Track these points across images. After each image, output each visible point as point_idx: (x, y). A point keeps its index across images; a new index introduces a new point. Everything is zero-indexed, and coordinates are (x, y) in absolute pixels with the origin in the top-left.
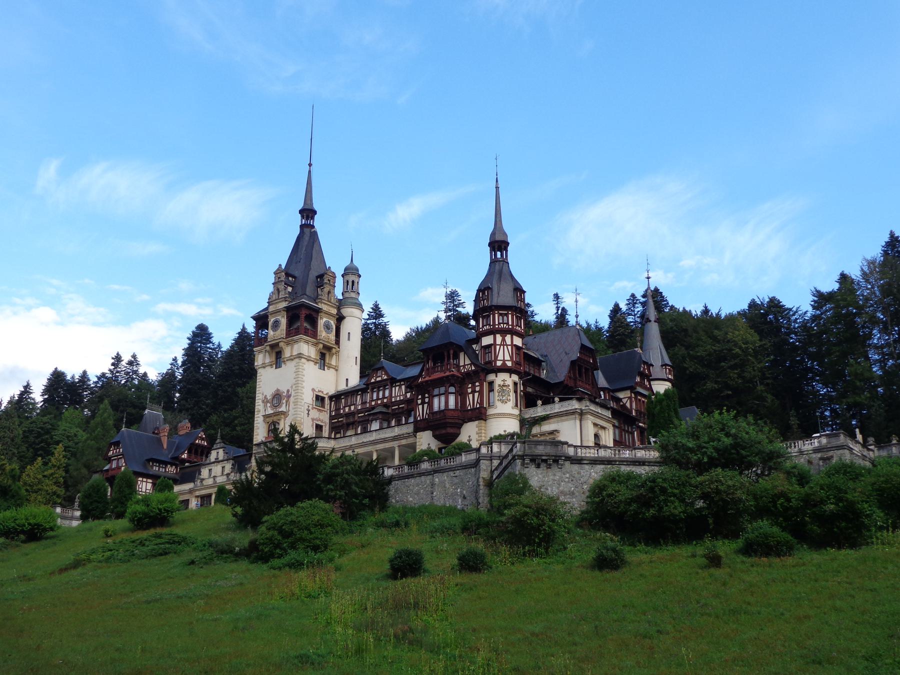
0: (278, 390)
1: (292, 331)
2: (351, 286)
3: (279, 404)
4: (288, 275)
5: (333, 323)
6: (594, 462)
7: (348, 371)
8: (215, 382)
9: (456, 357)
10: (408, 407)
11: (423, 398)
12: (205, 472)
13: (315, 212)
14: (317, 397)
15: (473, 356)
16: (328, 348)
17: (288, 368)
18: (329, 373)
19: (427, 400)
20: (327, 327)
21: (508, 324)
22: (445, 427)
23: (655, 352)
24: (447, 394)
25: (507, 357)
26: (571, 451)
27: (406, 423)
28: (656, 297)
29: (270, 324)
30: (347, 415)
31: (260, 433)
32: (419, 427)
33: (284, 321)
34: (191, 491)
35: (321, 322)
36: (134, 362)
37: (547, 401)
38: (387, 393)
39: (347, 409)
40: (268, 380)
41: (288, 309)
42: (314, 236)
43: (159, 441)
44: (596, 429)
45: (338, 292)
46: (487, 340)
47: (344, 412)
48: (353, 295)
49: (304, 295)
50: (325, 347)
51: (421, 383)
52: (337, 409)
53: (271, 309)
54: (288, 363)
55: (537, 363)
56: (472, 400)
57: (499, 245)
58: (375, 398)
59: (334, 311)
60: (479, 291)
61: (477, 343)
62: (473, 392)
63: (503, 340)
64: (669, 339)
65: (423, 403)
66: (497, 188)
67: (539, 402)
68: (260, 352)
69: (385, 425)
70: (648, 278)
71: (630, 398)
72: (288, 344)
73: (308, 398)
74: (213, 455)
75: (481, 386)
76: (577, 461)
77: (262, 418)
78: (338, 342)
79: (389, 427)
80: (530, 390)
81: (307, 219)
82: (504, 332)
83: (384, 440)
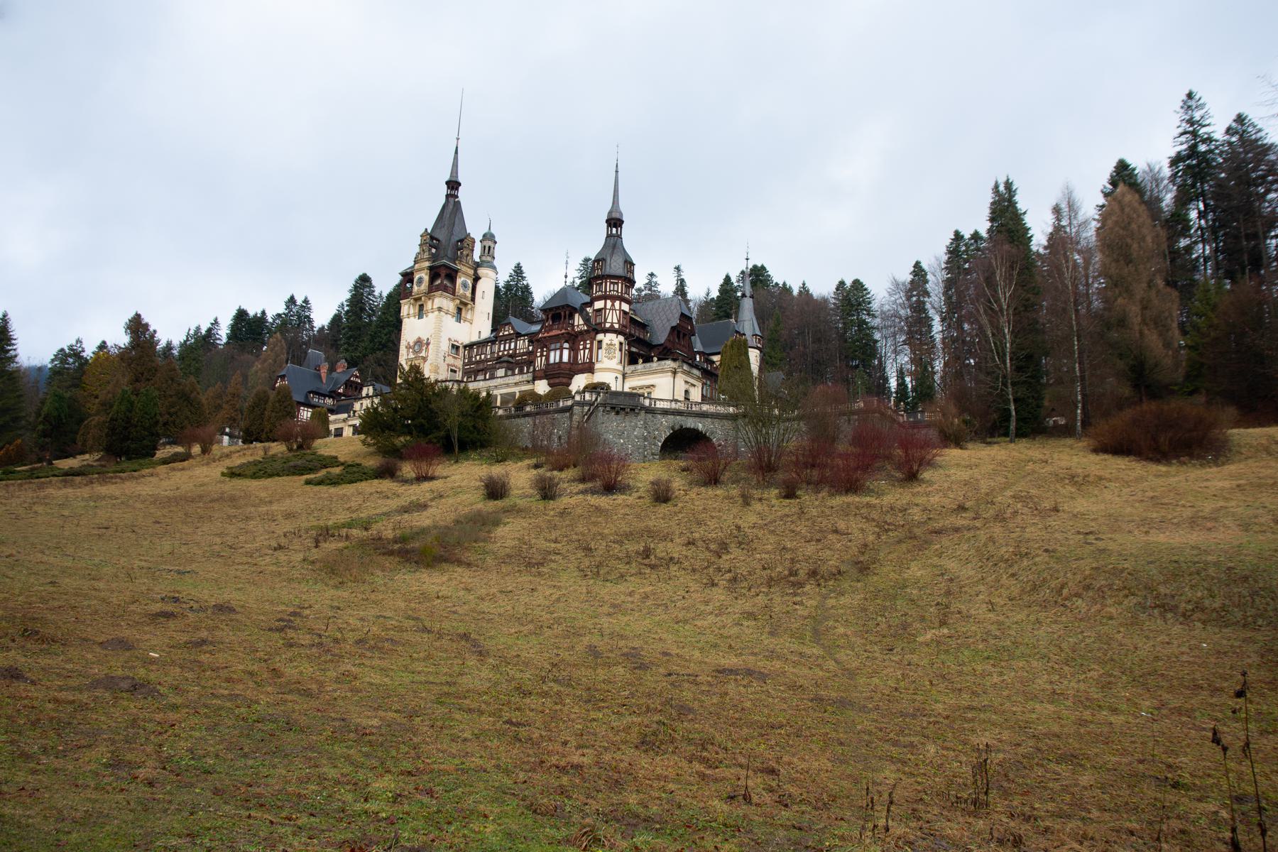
1: (432, 289)
2: (488, 251)
3: (420, 351)
4: (432, 238)
5: (470, 282)
6: (665, 412)
7: (479, 325)
8: (369, 328)
9: (571, 317)
14: (453, 346)
16: (466, 304)
17: (431, 318)
18: (464, 325)
20: (465, 285)
22: (559, 376)
23: (747, 322)
24: (561, 349)
25: (615, 320)
26: (647, 403)
28: (758, 276)
30: (477, 363)
33: (426, 278)
34: (344, 421)
35: (459, 281)
40: (413, 328)
41: (431, 268)
42: (458, 205)
43: (320, 377)
44: (687, 386)
46: (599, 305)
47: (476, 359)
48: (489, 259)
49: (447, 256)
50: (462, 303)
52: (470, 358)
54: (430, 315)
55: (643, 326)
56: (583, 355)
57: (615, 222)
58: (503, 349)
59: (472, 272)
62: (585, 348)
64: (761, 315)
73: (445, 347)
74: (364, 393)
75: (592, 344)
76: (651, 411)
78: (473, 299)
79: (514, 374)
80: (634, 349)
82: (613, 298)
83: (508, 385)
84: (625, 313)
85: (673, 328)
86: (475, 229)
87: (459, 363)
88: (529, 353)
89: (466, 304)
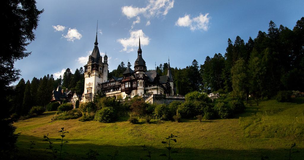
10: (120, 86)
11: (123, 85)
12: (72, 100)
13: (98, 44)
15: (134, 76)
16: (101, 73)
18: (101, 79)
25: (142, 76)
27: (119, 90)
31: (85, 92)
32: (122, 91)
35: (99, 68)
36: (52, 75)
37: (150, 86)
38: (114, 83)
41: (92, 65)
50: (100, 73)
52: (103, 87)
53: (88, 65)
55: (148, 78)
56: (134, 85)
57: (140, 52)
59: (102, 65)
60: (136, 62)
61: (135, 73)
62: (134, 84)
63: (141, 73)
65: (123, 86)
66: (140, 40)
67: (148, 86)
69: (114, 90)
70: (169, 60)
71: (166, 85)
72: (92, 72)
73: (97, 84)
74: (74, 97)
78: (103, 72)
79: (115, 91)
81: (96, 45)
82: (141, 71)
84: (144, 74)
86: (102, 54)
88: (118, 85)
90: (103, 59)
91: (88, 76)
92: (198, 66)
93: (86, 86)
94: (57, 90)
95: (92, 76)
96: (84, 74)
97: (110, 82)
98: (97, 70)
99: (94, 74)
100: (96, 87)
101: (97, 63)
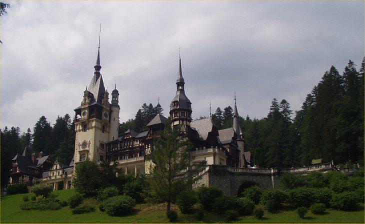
0: (85, 141)
5: (108, 114)
8: (54, 138)
16: (107, 124)
18: (105, 135)
19: (150, 147)
20: (106, 115)
21: (185, 116)
25: (184, 130)
29: (82, 113)
30: (113, 152)
31: (77, 158)
38: (131, 144)
39: (114, 150)
45: (110, 101)
46: (177, 123)
51: (148, 140)
57: (181, 84)
59: (108, 109)
60: (173, 102)
63: (183, 123)
65: (148, 148)
66: (180, 60)
67: (197, 149)
68: (77, 125)
73: (98, 145)
74: (54, 168)
77: (78, 152)
78: (109, 121)
79: (132, 157)
82: (183, 120)
83: (131, 163)
85: (209, 133)
86: (109, 89)
87: (104, 153)
88: (139, 147)
89: (107, 124)
90: (110, 97)
91: (81, 128)
92: (291, 111)
93: (78, 148)
94: (24, 155)
95: (88, 129)
96: (73, 126)
97: (124, 141)
98: (99, 117)
99: (94, 124)
100: (96, 150)
101: (99, 107)
